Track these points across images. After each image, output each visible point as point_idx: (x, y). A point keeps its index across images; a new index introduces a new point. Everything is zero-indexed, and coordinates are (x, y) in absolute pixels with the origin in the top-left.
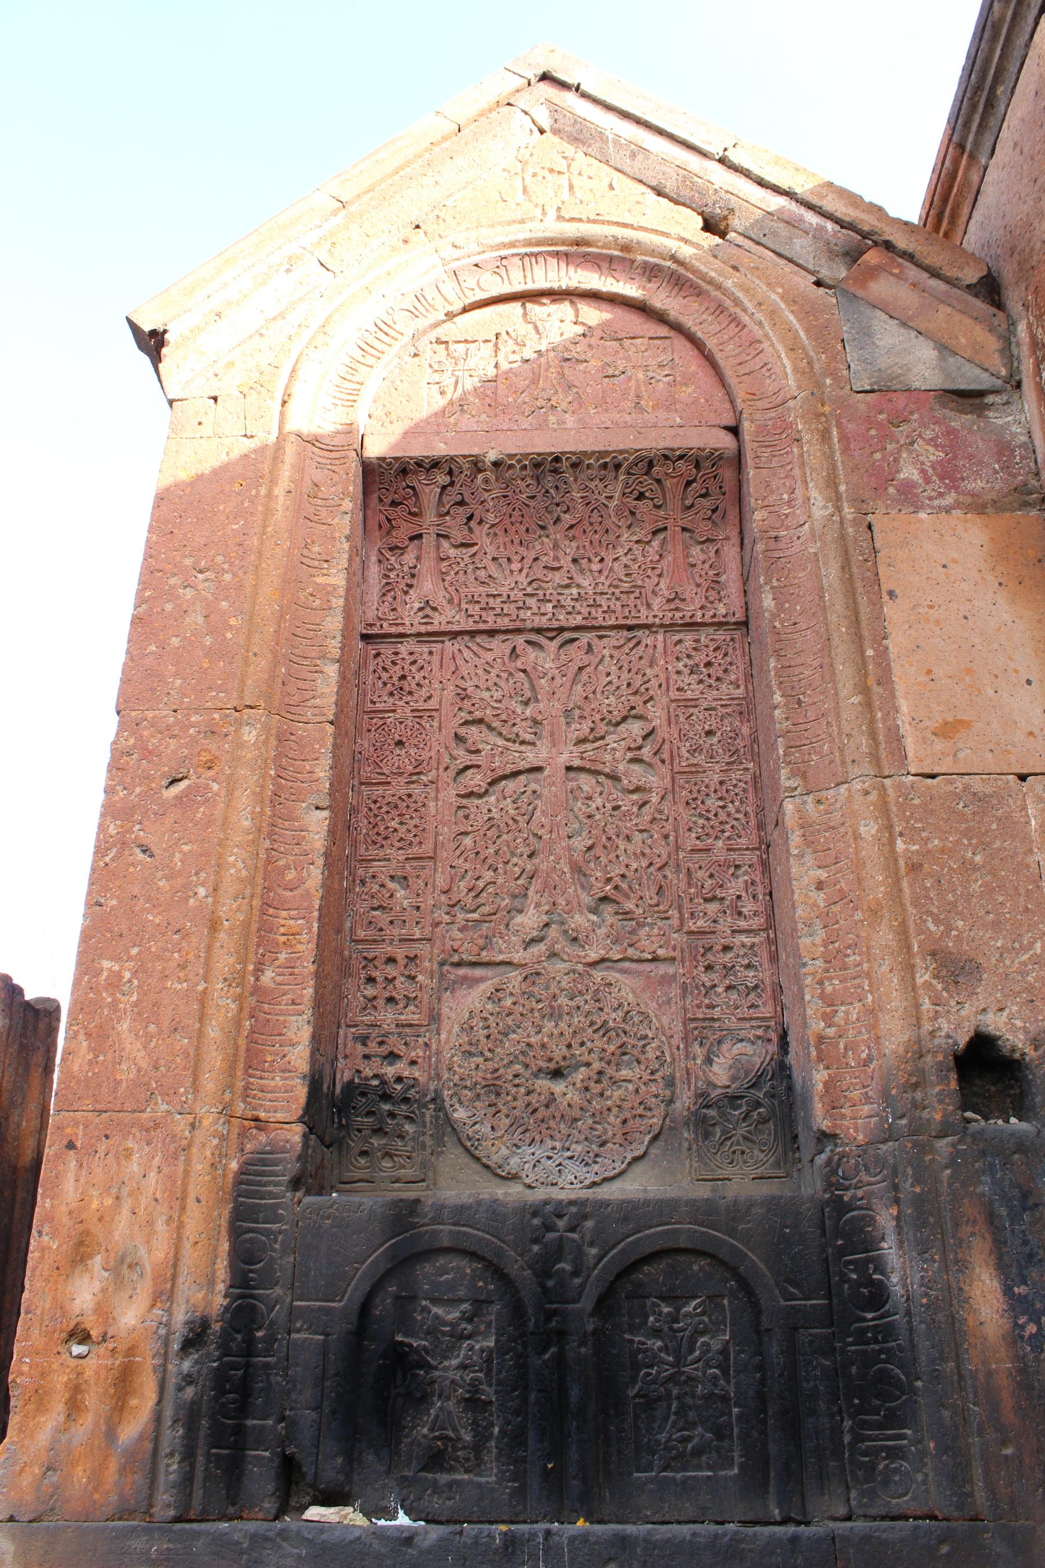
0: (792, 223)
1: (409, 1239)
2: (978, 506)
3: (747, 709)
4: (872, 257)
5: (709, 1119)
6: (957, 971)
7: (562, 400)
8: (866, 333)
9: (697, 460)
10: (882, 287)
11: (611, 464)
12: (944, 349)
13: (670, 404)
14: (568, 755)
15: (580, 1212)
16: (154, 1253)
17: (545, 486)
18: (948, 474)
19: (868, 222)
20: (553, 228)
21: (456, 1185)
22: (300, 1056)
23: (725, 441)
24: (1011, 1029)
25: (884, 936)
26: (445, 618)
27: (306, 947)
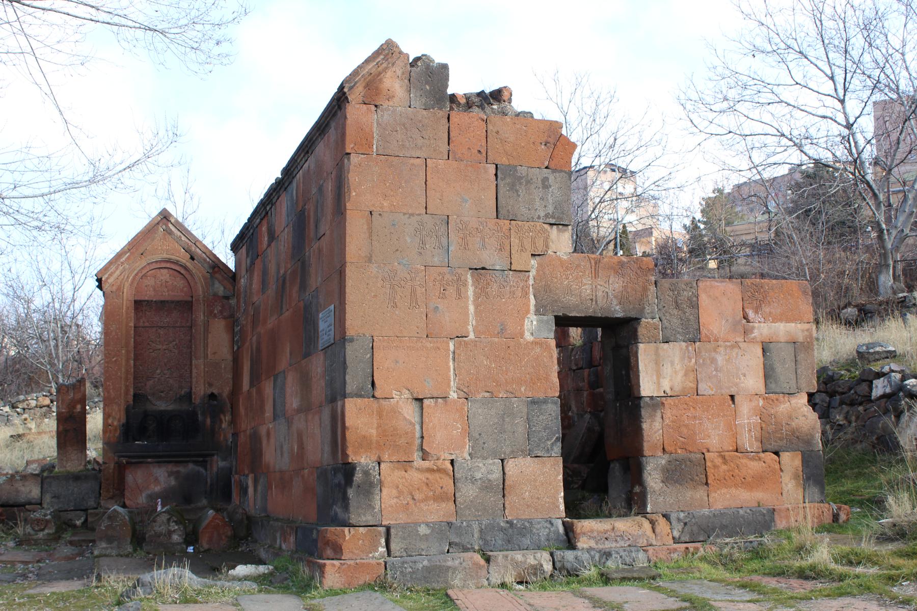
0: (205, 260)
1: (146, 414)
2: (225, 318)
3: (191, 341)
4: (216, 269)
5: (181, 399)
6: (210, 385)
7: (166, 290)
8: (213, 284)
9: (186, 302)
10: (217, 275)
11: (172, 302)
12: (225, 288)
13: (182, 291)
14: (164, 347)
15: (165, 411)
16: (118, 417)
17: (161, 305)
18: (221, 312)
19: (217, 262)
20: (165, 256)
21: (149, 407)
22: (132, 393)
23: (190, 299)
24: (216, 392)
25: (202, 381)
26: (147, 324)
27: (132, 379)
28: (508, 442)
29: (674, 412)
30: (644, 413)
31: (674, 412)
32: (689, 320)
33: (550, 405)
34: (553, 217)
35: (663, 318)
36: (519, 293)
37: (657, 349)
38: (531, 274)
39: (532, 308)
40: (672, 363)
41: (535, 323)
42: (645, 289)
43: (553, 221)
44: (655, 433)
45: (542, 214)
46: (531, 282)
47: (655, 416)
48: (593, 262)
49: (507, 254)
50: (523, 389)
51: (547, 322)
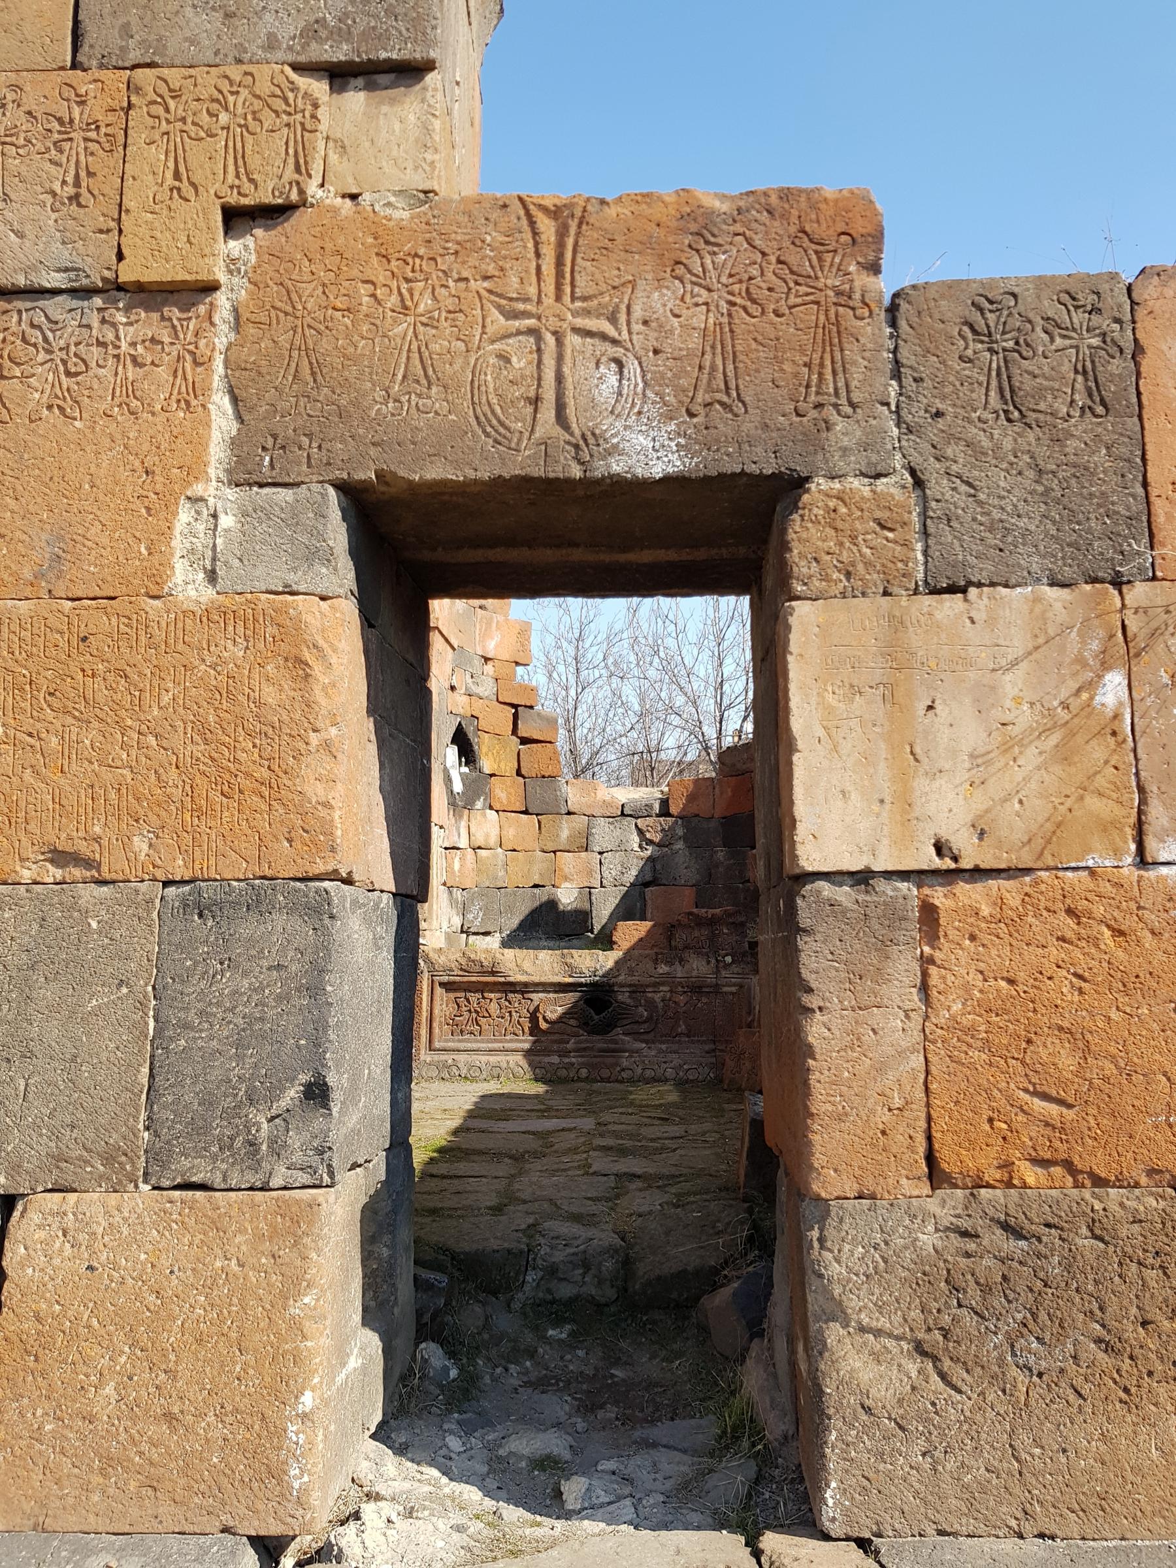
28: (38, 1108)
29: (998, 956)
30: (816, 960)
31: (998, 956)
32: (1084, 471)
33: (279, 920)
34: (342, 34)
35: (932, 471)
36: (159, 384)
37: (897, 623)
38: (222, 299)
39: (217, 453)
40: (984, 699)
41: (227, 521)
42: (833, 336)
43: (340, 53)
44: (880, 1069)
45: (288, 29)
46: (222, 336)
47: (880, 977)
48: (548, 227)
49: (96, 214)
50: (140, 845)
51: (292, 517)
